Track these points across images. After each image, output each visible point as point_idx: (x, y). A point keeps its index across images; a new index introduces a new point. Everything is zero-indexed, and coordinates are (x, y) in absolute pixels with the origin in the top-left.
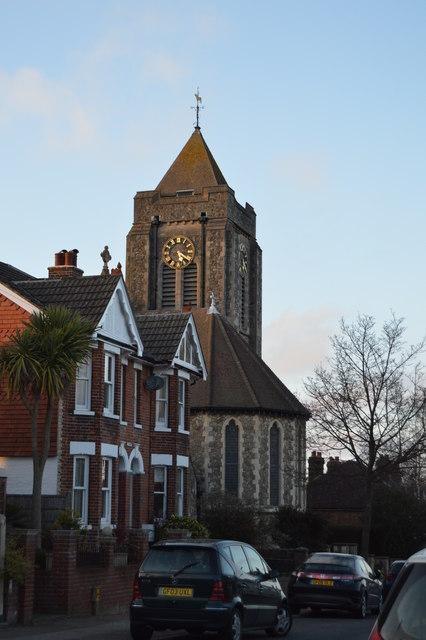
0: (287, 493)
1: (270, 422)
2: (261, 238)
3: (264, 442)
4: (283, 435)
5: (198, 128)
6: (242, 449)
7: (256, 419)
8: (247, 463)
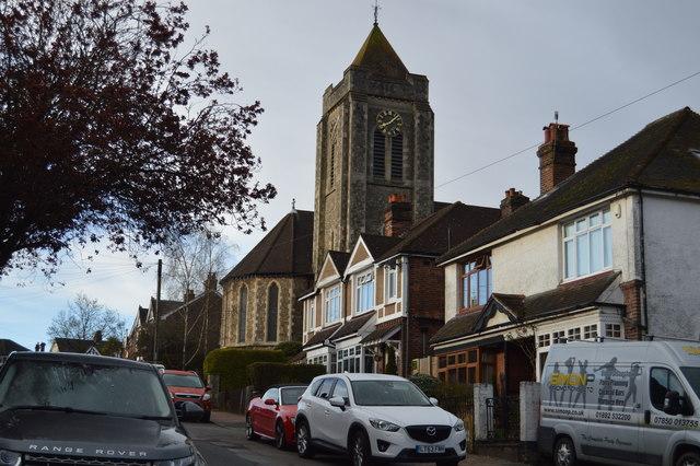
5: (376, 24)
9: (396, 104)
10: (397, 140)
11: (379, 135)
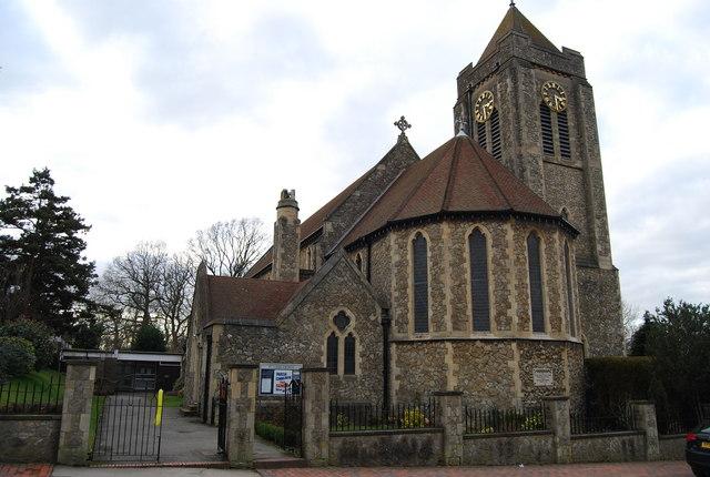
0: (500, 314)
1: (469, 229)
2: (591, 75)
3: (458, 253)
4: (490, 242)
5: (512, 4)
6: (430, 264)
7: (445, 228)
8: (435, 279)
9: (556, 76)
10: (562, 115)
11: (545, 108)
